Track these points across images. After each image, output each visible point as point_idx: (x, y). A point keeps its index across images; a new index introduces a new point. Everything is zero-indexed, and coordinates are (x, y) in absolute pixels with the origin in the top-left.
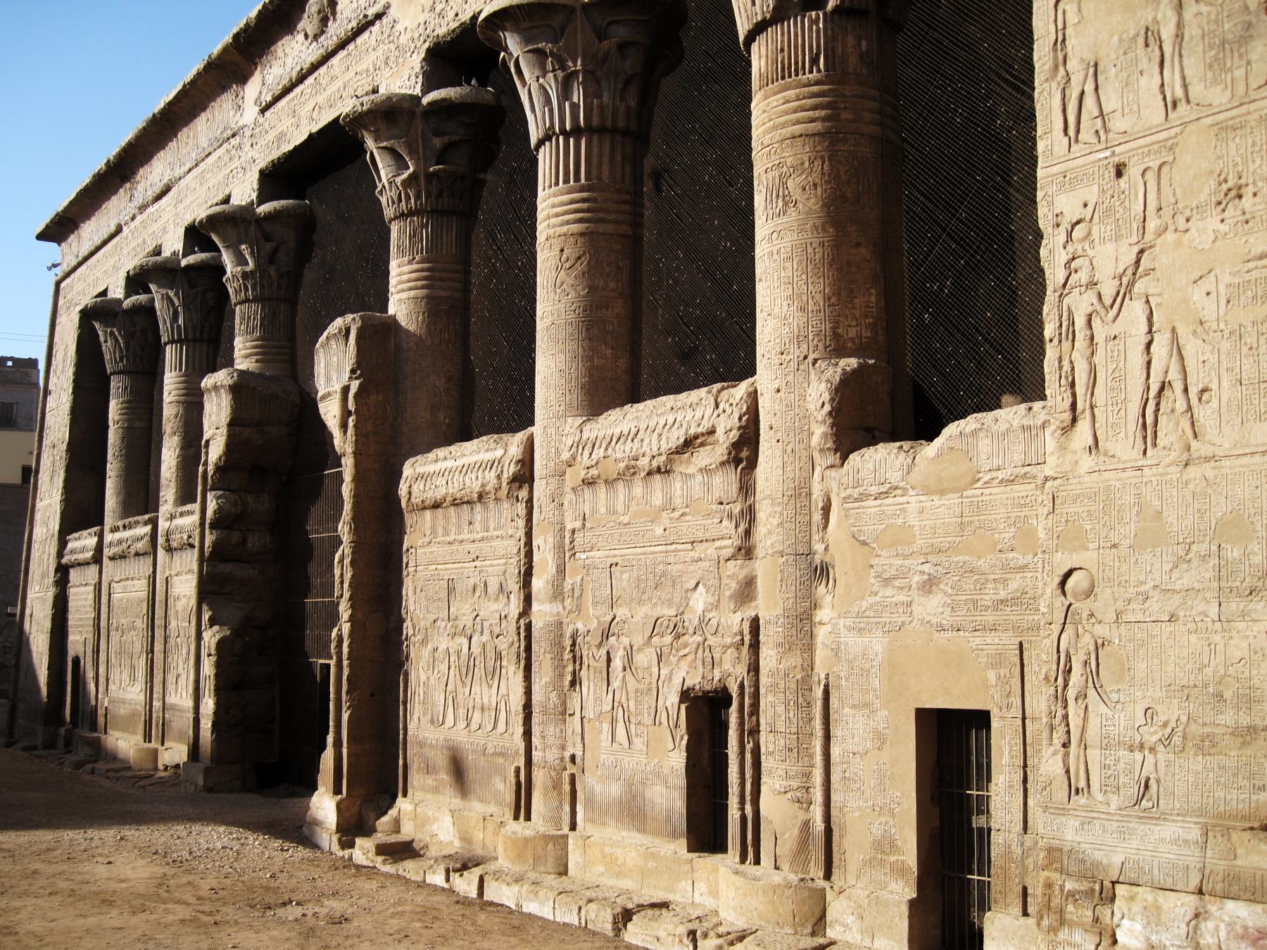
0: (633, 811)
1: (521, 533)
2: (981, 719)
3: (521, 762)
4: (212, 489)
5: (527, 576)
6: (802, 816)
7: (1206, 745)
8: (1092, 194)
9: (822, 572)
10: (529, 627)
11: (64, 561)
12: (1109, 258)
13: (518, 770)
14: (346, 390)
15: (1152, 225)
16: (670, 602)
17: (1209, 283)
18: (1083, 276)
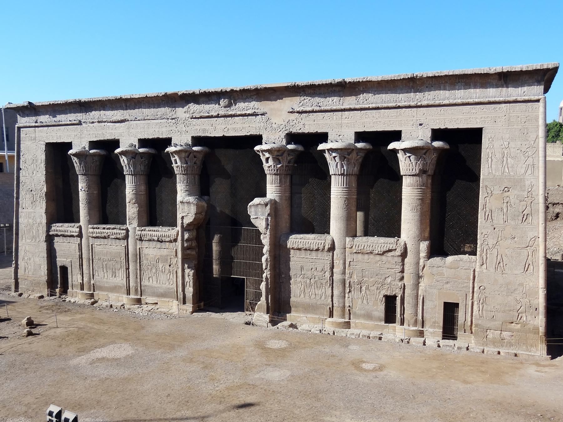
0: (368, 316)
1: (331, 259)
2: (457, 305)
3: (331, 306)
4: (186, 230)
5: (332, 268)
7: (504, 312)
8: (489, 231)
10: (333, 279)
11: (51, 233)
12: (491, 242)
13: (330, 308)
14: (267, 219)
15: (499, 239)
16: (381, 279)
17: (508, 249)
18: (486, 243)
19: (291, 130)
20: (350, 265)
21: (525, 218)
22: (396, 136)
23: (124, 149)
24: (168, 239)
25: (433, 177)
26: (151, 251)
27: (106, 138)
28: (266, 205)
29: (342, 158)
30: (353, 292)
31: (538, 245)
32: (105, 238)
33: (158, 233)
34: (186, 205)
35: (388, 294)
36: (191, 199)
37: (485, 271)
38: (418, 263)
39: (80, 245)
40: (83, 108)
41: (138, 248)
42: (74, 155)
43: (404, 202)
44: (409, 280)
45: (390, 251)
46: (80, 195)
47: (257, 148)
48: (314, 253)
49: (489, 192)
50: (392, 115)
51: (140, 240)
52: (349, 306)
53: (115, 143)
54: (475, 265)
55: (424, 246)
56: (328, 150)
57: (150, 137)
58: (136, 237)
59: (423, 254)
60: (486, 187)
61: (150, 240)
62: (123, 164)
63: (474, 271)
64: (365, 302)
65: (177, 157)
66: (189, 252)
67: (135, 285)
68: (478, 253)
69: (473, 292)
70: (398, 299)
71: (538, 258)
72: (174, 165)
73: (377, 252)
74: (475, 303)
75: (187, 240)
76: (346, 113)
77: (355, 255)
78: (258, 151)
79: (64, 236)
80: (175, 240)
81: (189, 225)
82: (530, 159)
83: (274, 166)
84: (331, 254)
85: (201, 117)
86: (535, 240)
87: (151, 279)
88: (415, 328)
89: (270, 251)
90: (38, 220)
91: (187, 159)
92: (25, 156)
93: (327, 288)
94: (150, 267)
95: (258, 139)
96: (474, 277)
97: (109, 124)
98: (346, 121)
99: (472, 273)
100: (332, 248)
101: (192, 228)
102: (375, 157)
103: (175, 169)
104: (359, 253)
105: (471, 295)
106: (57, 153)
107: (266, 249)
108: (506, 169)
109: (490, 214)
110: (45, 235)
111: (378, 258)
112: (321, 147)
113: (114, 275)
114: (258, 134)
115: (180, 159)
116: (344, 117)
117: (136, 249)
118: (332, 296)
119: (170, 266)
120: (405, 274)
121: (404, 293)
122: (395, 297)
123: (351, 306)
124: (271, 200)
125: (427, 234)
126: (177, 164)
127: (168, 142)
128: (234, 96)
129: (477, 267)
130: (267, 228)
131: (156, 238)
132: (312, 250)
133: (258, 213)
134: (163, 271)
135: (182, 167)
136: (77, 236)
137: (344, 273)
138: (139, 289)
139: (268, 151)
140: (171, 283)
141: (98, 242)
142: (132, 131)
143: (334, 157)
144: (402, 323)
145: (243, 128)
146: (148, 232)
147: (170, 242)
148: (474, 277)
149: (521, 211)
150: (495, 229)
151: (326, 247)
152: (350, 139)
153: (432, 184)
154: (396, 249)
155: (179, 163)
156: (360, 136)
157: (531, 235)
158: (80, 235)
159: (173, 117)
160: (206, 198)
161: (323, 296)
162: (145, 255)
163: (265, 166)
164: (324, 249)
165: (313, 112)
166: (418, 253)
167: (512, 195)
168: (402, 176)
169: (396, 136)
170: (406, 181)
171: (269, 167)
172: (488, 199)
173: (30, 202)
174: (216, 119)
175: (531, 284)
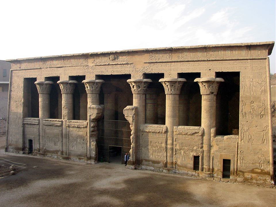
1: (166, 137)
4: (91, 122)
6: (208, 167)
9: (212, 146)
14: (133, 117)
18: (243, 129)
19: (145, 72)
20: (175, 140)
21: (262, 116)
22: (198, 75)
23: (62, 81)
24: (83, 127)
25: (217, 96)
27: (53, 76)
28: (133, 109)
29: (171, 86)
30: (177, 155)
31: (269, 130)
32: (50, 125)
33: (77, 123)
34: (92, 109)
35: (195, 154)
36: (94, 106)
37: (243, 143)
38: (210, 139)
39: (39, 129)
40: (43, 61)
41: (67, 131)
42: (37, 84)
43: (202, 108)
44: (205, 148)
45: (196, 133)
46: (39, 104)
47: (128, 81)
48: (157, 135)
49: (244, 103)
50: (196, 65)
52: (175, 162)
53: (58, 78)
54: (238, 140)
55: (213, 130)
56: (164, 82)
57: (75, 75)
58: (67, 125)
59: (212, 135)
60: (243, 101)
61: (73, 127)
62: (61, 89)
63: (238, 142)
64: (183, 159)
65: (88, 85)
66: (93, 133)
68: (239, 134)
69: (238, 154)
70: (200, 158)
71: (269, 137)
72: (86, 89)
73: (189, 134)
74: (239, 159)
75: (92, 127)
76: (173, 63)
77: (179, 135)
78: (129, 82)
79: (31, 124)
80: (86, 127)
81: (93, 119)
82: (263, 87)
83: (137, 90)
84: (166, 135)
85: (100, 65)
86: (267, 127)
87: (74, 147)
88: (208, 173)
89: (135, 133)
90: (19, 117)
91: (93, 86)
92: (14, 85)
93: (164, 152)
95: (129, 76)
96: (238, 146)
97: (55, 68)
98: (173, 68)
99: (237, 144)
100: (166, 132)
101: (94, 121)
102: (188, 85)
103: (87, 91)
104: (180, 134)
105: (236, 155)
106: (30, 82)
107: (132, 133)
108: (252, 92)
109: (245, 114)
110: (22, 124)
111: (190, 137)
112: (160, 80)
113: (55, 144)
114: (129, 73)
115: (89, 86)
116: (172, 65)
118: (167, 157)
120: (204, 145)
121: (203, 154)
122: (198, 157)
123: (176, 161)
124: (135, 107)
125: (214, 125)
126: (88, 88)
127: (83, 77)
128: (117, 54)
129: (239, 141)
130: (133, 121)
131: (76, 126)
132: (156, 133)
133: (128, 113)
134: (80, 143)
135: (90, 90)
136: (37, 125)
137: (173, 144)
138: (68, 152)
139: (134, 82)
140: (84, 149)
141: (47, 128)
142: (66, 72)
143: (167, 85)
144: (202, 170)
145: (121, 71)
146: (73, 123)
147: (84, 128)
148: (238, 146)
149: (260, 113)
150: (247, 122)
151: (163, 131)
152: (175, 77)
153: (217, 99)
154: (199, 132)
155: (89, 88)
156: (180, 75)
157: (265, 125)
158: (39, 124)
159: (86, 65)
160: (101, 105)
161: (162, 156)
162: (71, 134)
163: (132, 89)
164: (162, 132)
165: (156, 63)
166: (210, 134)
167: (255, 105)
168: (201, 95)
169: (198, 75)
170: (203, 98)
171: (134, 90)
172: (243, 108)
173: (15, 107)
174: (108, 66)
175: (266, 149)
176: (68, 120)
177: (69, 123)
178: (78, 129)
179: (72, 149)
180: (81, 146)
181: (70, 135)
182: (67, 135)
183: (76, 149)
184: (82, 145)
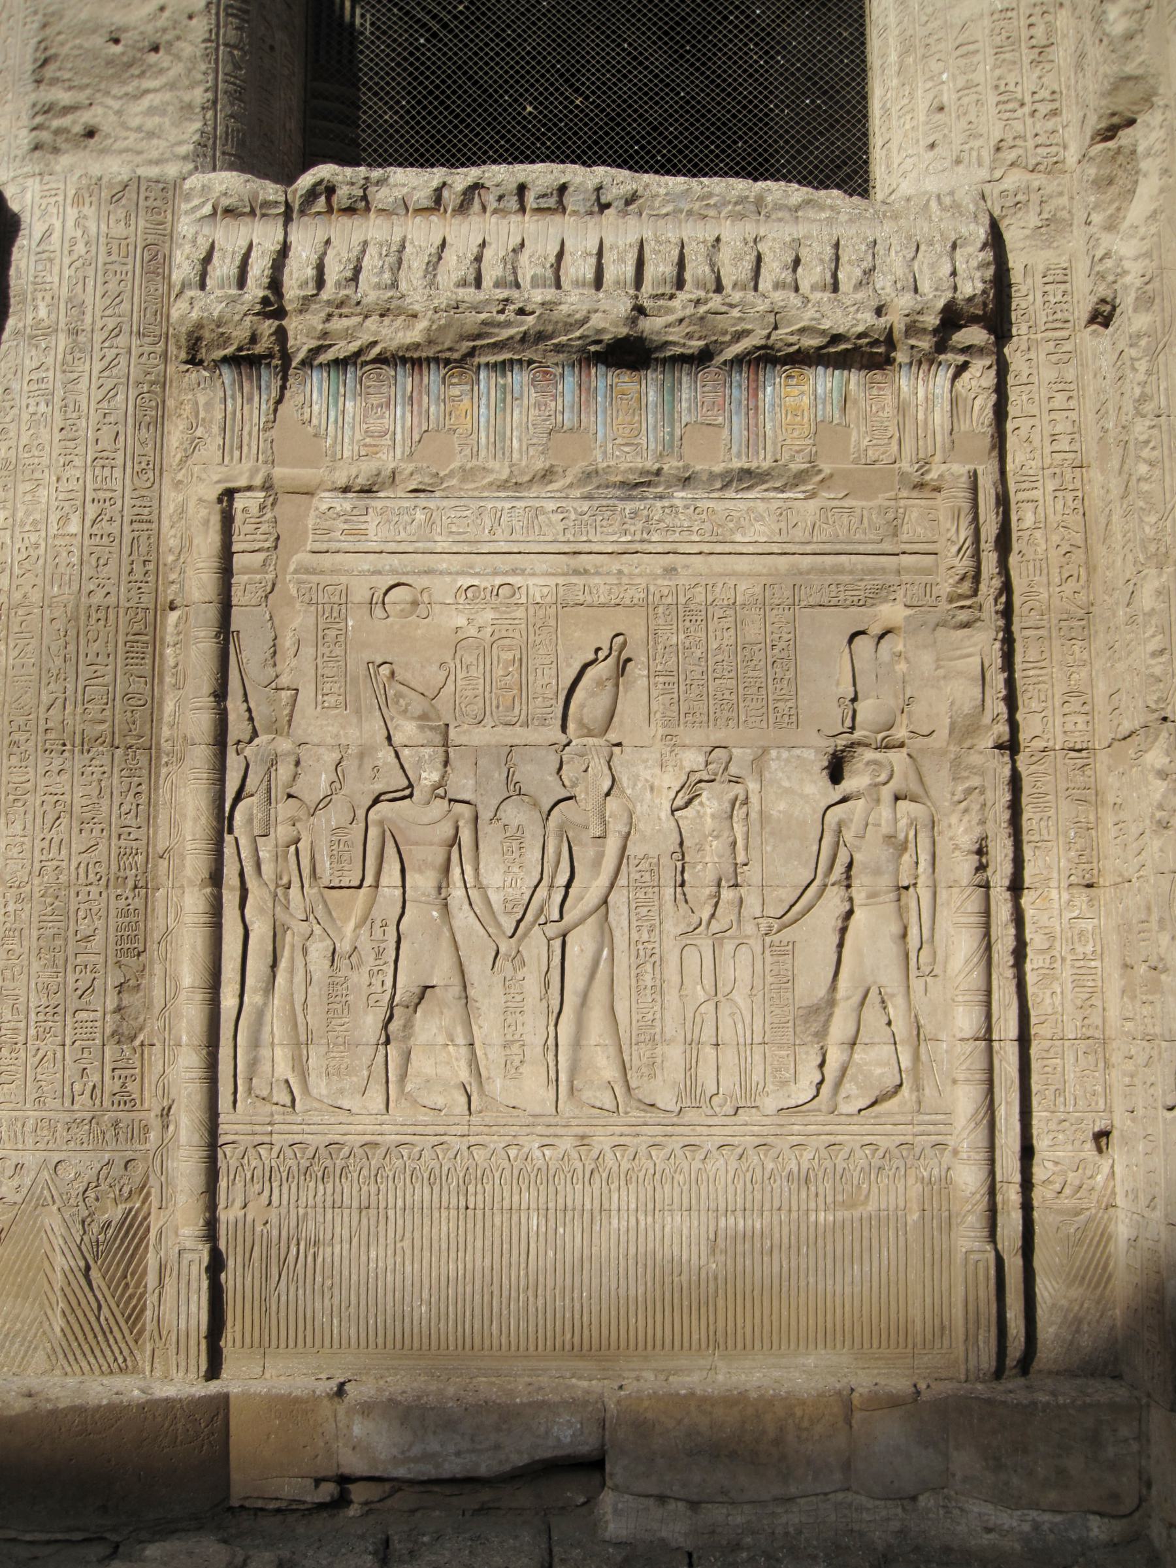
26: (456, 541)
51: (245, 361)
58: (185, 311)
67: (82, 1164)
87: (430, 1027)
94: (424, 821)
117: (146, 520)
119: (836, 771)
138: (177, 1227)
140: (877, 1063)
146: (422, 234)
147: (868, 355)
162: (332, 611)
176: (207, 155)
177: (265, 237)
178: (625, 421)
179: (346, 1105)
180: (741, 968)
181: (298, 621)
182: (145, 642)
183: (533, 1090)
184: (789, 917)
